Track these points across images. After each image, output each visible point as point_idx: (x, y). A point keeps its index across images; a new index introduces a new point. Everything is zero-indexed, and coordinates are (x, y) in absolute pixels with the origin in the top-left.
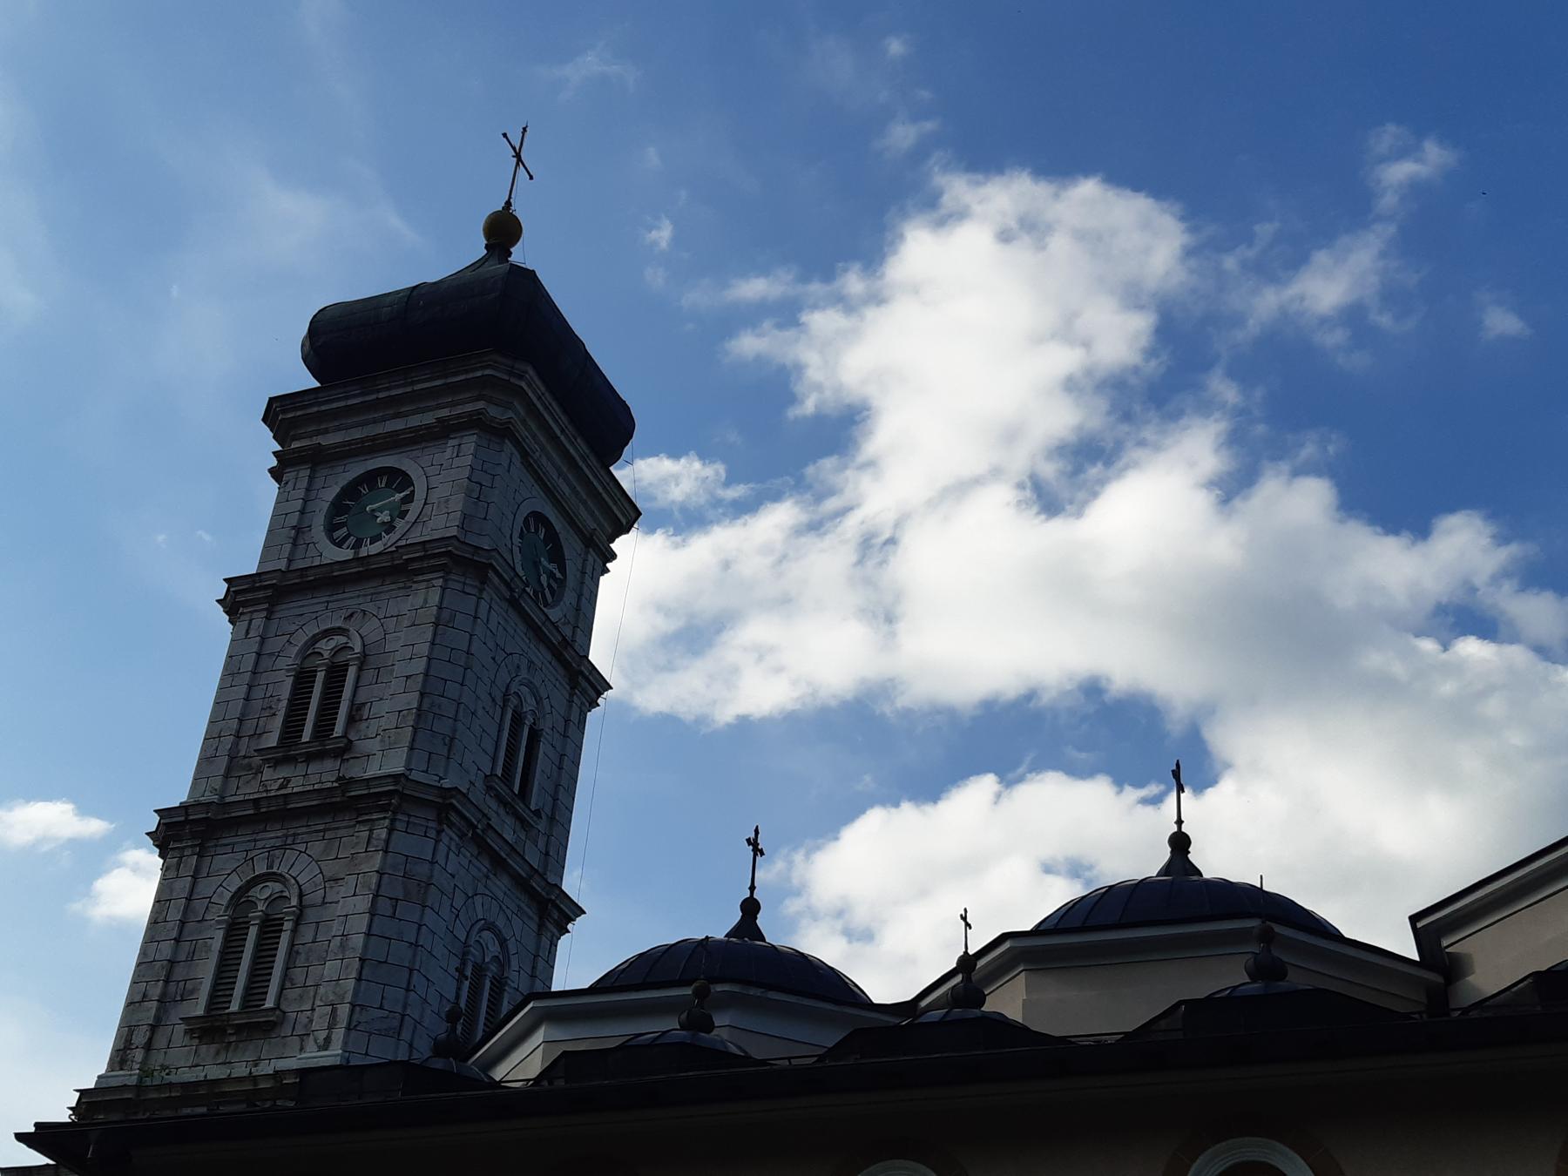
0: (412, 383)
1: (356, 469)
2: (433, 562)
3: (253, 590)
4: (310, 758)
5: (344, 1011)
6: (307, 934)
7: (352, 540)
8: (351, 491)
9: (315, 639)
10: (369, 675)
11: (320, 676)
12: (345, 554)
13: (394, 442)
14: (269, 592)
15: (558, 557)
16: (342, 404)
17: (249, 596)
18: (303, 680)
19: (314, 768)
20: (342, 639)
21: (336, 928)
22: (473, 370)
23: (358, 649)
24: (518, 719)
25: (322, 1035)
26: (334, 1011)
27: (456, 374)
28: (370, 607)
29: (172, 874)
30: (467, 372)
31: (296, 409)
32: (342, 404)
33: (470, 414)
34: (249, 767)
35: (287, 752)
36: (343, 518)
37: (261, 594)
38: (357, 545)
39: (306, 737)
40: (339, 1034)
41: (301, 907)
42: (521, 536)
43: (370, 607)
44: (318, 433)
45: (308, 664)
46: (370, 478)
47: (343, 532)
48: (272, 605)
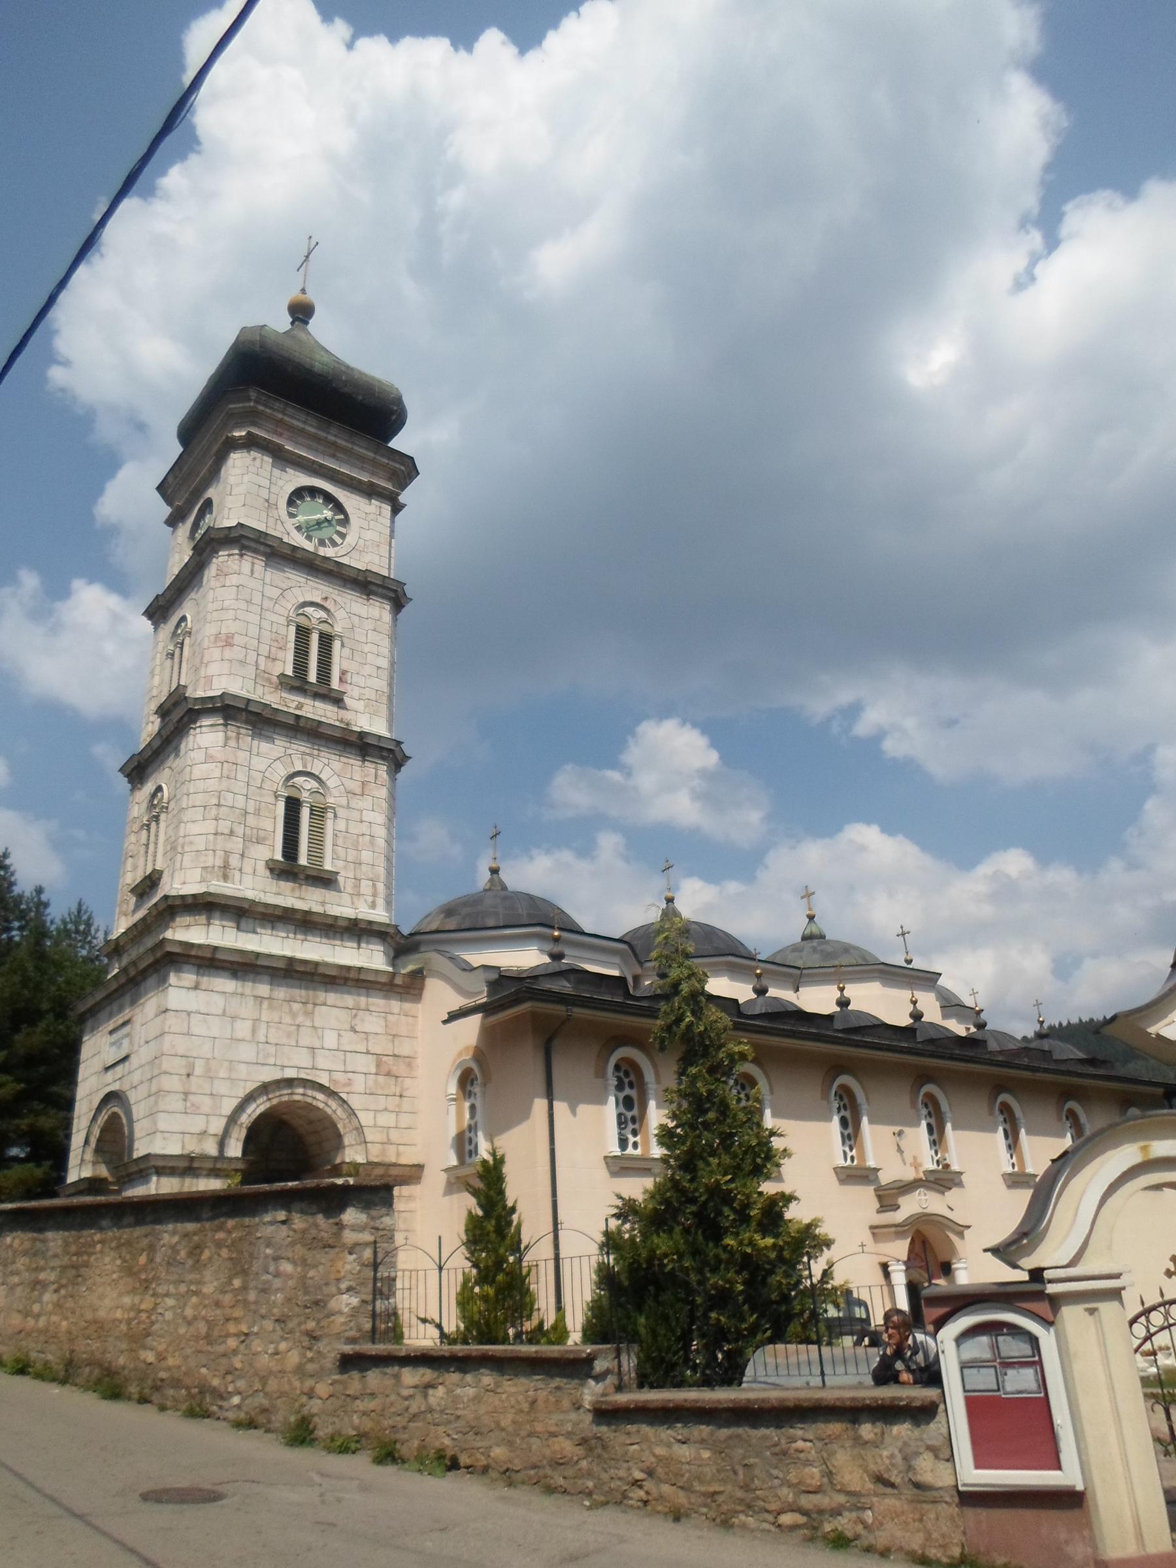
0: (353, 443)
2: (384, 591)
3: (257, 541)
4: (317, 696)
5: (381, 887)
6: (341, 825)
8: (298, 494)
11: (315, 637)
12: (309, 546)
14: (268, 550)
16: (301, 425)
17: (253, 545)
18: (303, 633)
19: (317, 704)
21: (364, 828)
22: (394, 461)
25: (370, 899)
26: (374, 886)
27: (383, 456)
28: (338, 599)
29: (232, 743)
30: (389, 459)
31: (265, 406)
32: (301, 425)
33: (393, 492)
34: (269, 680)
35: (297, 683)
37: (262, 548)
39: (312, 677)
40: (380, 902)
43: (338, 599)
44: (275, 432)
45: (302, 621)
46: (313, 491)
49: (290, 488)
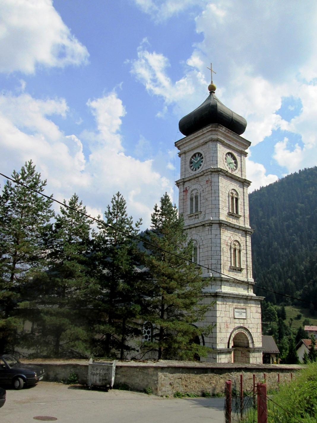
1: (192, 153)
7: (194, 169)
9: (192, 191)
10: (202, 198)
13: (198, 147)
15: (234, 159)
18: (191, 199)
20: (196, 191)
23: (199, 193)
24: (232, 198)
36: (192, 165)
38: (196, 170)
39: (194, 212)
41: (200, 246)
42: (226, 159)
46: (195, 155)
47: (192, 167)
48: (183, 185)
49: (189, 160)
